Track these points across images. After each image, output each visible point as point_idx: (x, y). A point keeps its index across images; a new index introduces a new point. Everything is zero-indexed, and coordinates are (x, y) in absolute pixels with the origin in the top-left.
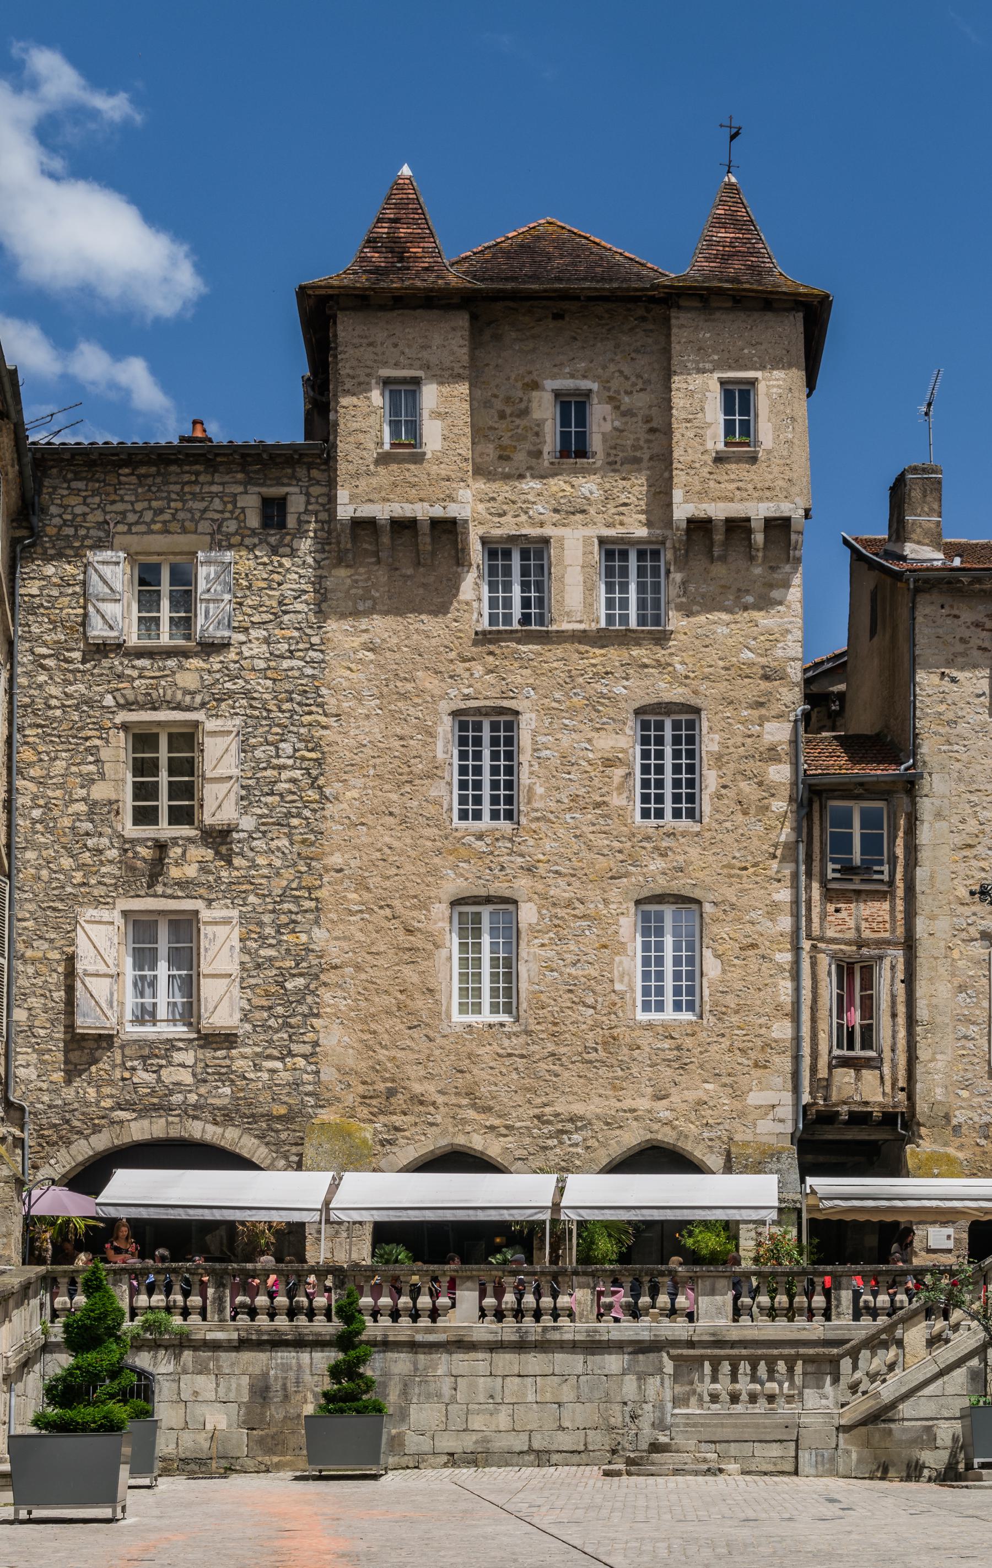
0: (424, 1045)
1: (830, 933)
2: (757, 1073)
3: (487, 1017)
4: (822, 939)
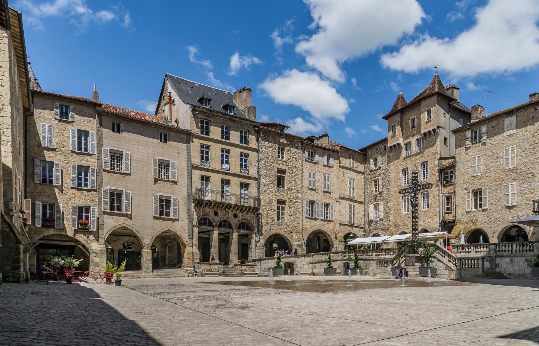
0: (400, 217)
1: (445, 193)
2: (435, 216)
3: (407, 212)
4: (444, 194)
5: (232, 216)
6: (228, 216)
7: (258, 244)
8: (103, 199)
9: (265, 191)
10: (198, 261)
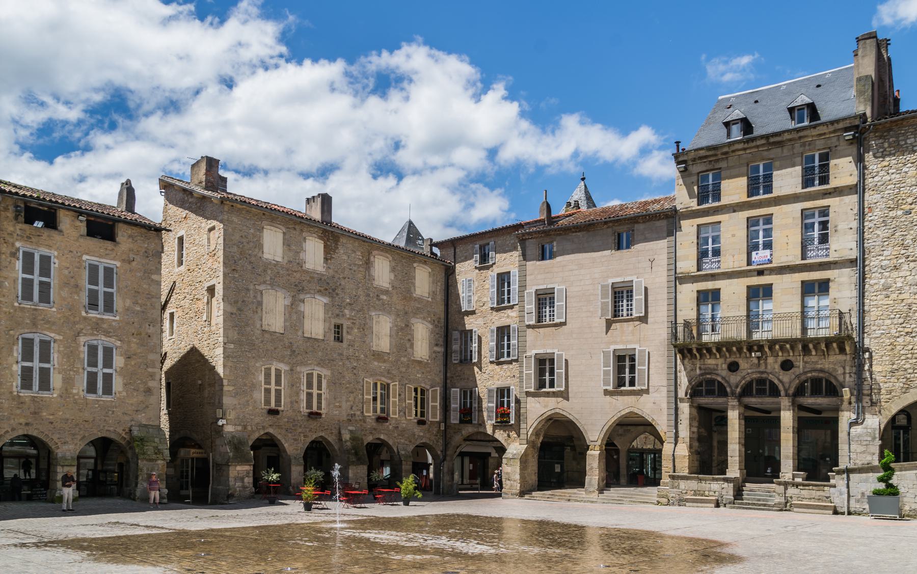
5: (777, 367)
6: (766, 368)
7: (857, 430)
8: (525, 372)
9: (886, 288)
10: (686, 472)
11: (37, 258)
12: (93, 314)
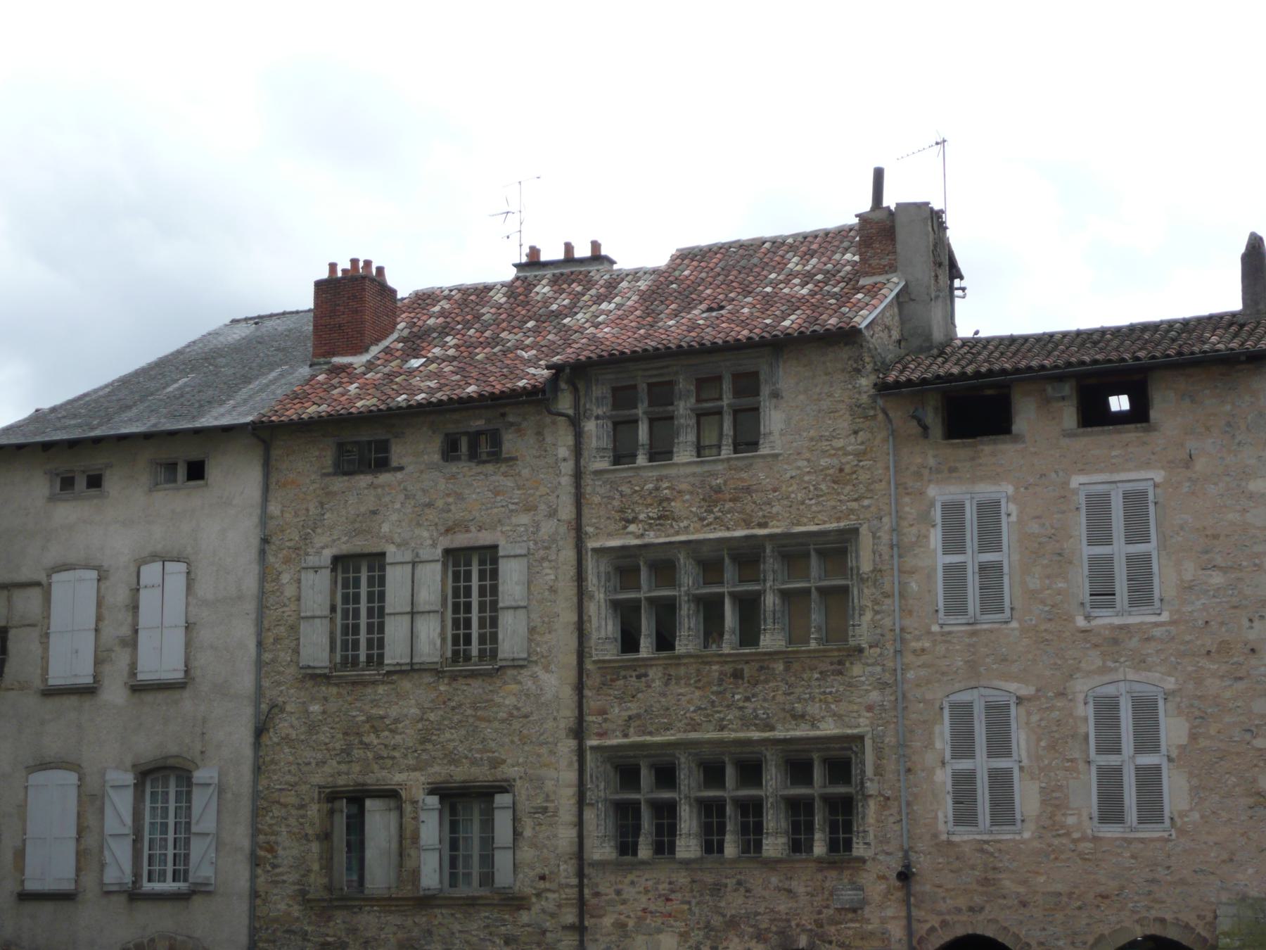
11: (970, 514)
12: (1106, 619)
